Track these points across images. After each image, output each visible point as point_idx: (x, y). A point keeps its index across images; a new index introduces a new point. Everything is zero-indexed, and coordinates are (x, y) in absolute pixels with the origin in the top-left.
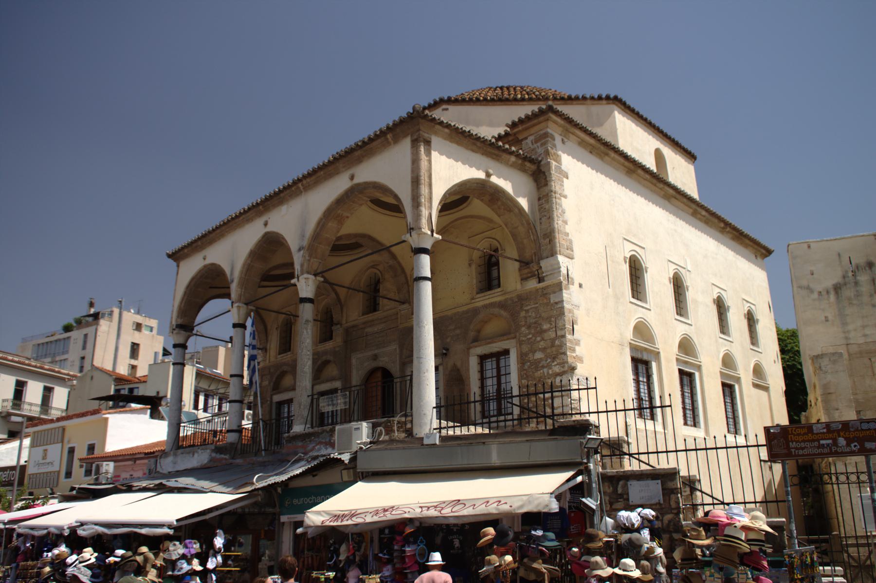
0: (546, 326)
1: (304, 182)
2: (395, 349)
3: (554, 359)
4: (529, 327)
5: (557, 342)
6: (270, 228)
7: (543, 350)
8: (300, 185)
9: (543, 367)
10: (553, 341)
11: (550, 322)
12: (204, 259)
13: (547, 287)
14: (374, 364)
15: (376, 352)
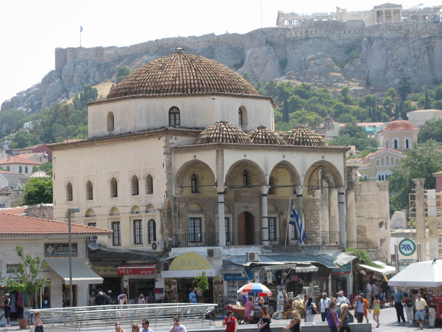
0: (314, 212)
1: (305, 149)
2: (256, 206)
3: (316, 224)
4: (309, 211)
5: (318, 219)
6: (286, 159)
7: (313, 220)
8: (303, 149)
9: (313, 226)
10: (316, 218)
11: (316, 211)
12: (245, 156)
13: (315, 199)
14: (246, 210)
15: (247, 205)
